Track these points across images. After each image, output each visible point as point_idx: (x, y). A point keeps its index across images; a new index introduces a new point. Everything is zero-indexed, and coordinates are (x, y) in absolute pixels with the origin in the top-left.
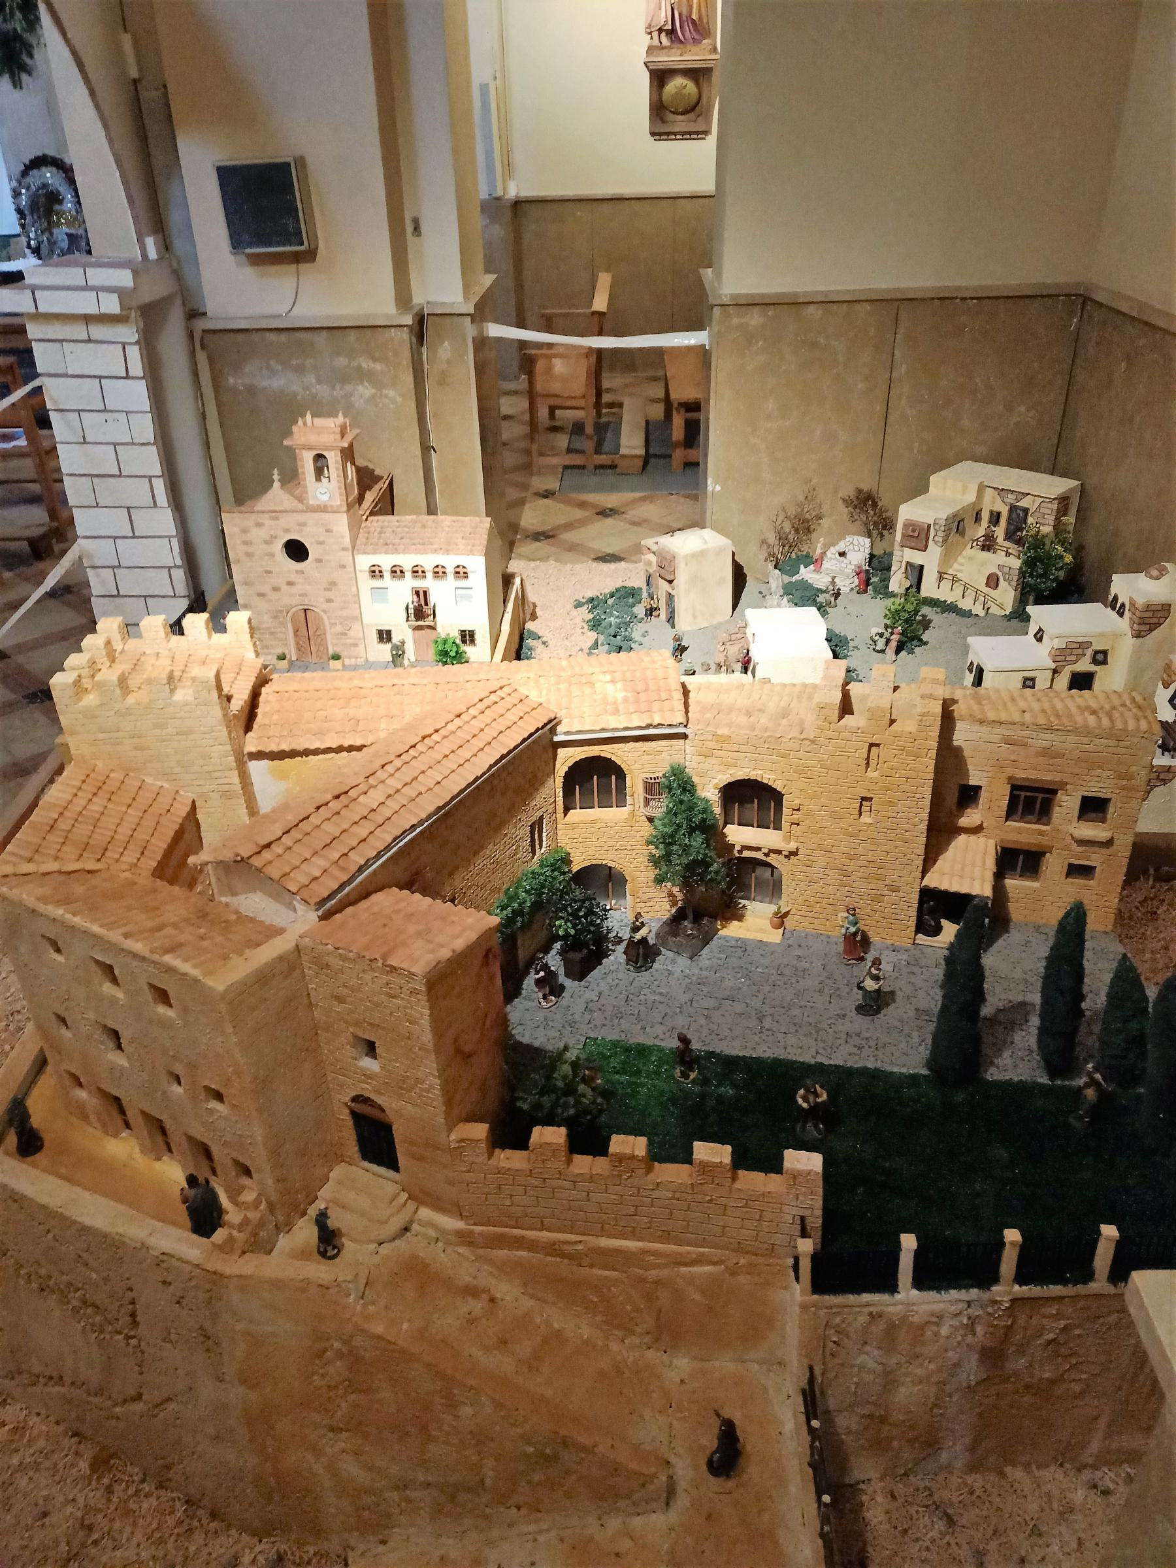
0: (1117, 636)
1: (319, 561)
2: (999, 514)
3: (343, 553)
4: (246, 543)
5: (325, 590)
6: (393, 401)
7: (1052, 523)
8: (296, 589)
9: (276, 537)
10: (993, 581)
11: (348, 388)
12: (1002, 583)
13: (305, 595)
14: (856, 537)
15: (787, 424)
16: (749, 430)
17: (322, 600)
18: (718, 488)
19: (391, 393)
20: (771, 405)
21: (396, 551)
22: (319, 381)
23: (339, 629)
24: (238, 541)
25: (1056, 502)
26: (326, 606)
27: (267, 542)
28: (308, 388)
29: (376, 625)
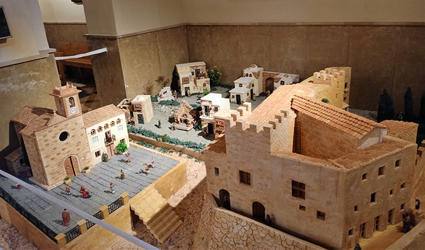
0: (253, 80)
1: (73, 136)
2: (193, 72)
3: (82, 130)
4: (46, 141)
5: (76, 146)
6: (43, 84)
7: (205, 70)
8: (66, 150)
9: (57, 134)
10: (204, 85)
11: (26, 83)
12: (207, 85)
13: (70, 151)
14: (166, 87)
15: (140, 65)
16: (132, 69)
17: (76, 150)
18: (128, 86)
19: (43, 81)
20: (135, 62)
21: (98, 122)
22: (14, 85)
23: (83, 158)
24: (43, 141)
26: (77, 152)
27: (53, 137)
28: (9, 88)
29: (94, 152)
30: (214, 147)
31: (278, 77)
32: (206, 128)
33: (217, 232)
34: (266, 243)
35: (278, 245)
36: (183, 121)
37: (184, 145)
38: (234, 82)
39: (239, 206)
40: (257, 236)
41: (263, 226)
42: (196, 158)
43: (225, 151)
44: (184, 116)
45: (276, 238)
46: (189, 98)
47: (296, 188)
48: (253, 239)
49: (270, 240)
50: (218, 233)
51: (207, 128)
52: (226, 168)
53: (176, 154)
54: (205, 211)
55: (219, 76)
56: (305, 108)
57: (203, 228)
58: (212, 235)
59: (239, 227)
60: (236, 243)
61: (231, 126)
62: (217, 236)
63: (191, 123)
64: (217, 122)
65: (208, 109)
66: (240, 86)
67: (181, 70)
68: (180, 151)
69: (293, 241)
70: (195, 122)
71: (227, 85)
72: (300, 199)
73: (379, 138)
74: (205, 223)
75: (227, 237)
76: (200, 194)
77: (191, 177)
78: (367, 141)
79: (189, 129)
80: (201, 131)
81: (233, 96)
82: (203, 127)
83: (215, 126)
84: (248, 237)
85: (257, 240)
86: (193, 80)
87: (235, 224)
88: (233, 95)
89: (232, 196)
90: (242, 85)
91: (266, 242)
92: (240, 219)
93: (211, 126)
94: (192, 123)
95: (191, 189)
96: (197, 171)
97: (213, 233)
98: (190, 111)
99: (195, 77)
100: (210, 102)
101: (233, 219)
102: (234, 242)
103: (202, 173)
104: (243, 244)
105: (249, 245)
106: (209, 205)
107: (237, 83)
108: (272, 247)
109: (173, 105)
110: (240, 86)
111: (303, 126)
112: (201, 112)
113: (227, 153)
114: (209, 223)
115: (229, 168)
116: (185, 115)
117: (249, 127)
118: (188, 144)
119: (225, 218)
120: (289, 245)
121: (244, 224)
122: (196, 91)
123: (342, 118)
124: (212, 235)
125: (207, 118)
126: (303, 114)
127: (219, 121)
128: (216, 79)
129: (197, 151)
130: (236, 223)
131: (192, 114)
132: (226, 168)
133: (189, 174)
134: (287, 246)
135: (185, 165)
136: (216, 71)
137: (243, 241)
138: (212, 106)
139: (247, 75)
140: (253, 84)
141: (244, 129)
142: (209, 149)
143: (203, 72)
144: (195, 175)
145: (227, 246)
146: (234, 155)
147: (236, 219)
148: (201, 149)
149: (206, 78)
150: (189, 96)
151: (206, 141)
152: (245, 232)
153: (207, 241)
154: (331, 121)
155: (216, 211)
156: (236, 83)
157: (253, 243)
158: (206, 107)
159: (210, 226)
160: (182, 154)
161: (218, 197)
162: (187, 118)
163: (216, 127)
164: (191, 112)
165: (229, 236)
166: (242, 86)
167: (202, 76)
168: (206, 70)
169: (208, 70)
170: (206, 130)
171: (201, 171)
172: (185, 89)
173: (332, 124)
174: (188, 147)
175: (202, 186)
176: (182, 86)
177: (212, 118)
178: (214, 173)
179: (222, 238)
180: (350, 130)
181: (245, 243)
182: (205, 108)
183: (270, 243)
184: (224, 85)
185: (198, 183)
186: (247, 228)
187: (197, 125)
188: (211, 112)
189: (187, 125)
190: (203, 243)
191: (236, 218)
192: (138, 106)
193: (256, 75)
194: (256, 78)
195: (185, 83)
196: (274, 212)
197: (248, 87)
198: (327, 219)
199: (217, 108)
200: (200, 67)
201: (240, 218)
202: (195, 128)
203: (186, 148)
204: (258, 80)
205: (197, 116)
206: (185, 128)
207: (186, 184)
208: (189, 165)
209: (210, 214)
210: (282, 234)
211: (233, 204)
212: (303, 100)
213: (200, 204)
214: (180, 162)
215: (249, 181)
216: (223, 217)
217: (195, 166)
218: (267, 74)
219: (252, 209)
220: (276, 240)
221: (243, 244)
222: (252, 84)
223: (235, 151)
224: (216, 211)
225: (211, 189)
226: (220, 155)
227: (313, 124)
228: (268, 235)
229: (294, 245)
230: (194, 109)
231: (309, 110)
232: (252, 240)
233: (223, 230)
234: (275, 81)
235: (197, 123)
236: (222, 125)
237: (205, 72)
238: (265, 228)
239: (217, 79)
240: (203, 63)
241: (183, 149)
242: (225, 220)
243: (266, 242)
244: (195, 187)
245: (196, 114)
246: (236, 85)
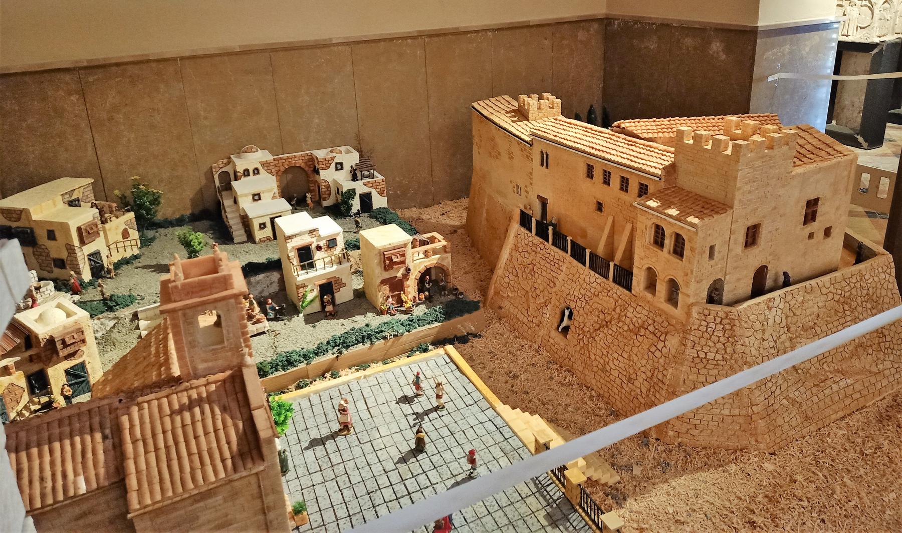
10: (125, 234)
12: (130, 231)
66: (254, 200)
67: (42, 212)
75: (764, 340)
81: (260, 225)
84: (787, 317)
87: (767, 312)
88: (261, 222)
92: (770, 299)
100: (312, 232)
107: (246, 195)
109: (117, 307)
110: (254, 200)
127: (393, 254)
138: (321, 239)
152: (782, 313)
166: (260, 199)
172: (89, 259)
174: (347, 347)
176: (79, 254)
192: (75, 336)
193: (269, 168)
195: (90, 240)
199: (335, 239)
200: (79, 192)
218: (280, 161)
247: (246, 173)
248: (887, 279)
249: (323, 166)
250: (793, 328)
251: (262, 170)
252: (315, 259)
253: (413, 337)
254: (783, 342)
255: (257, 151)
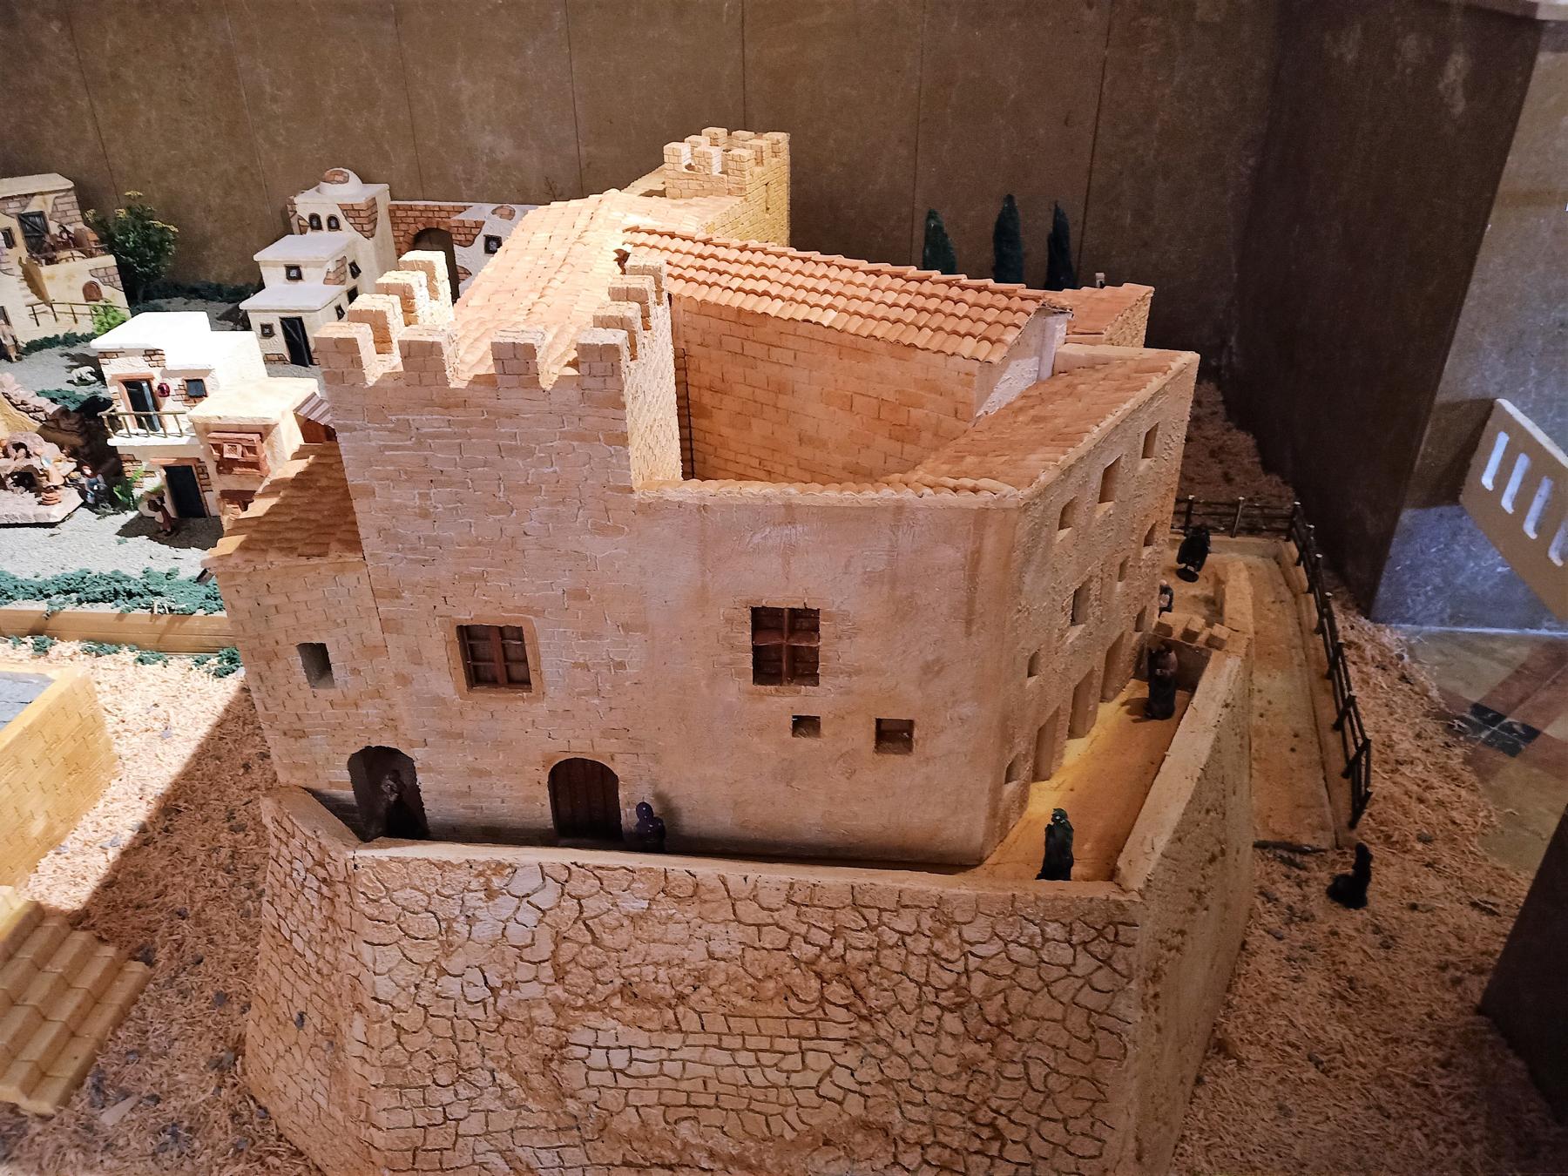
7: (80, 218)
10: (91, 292)
25: (72, 193)
30: (269, 532)
31: (468, 217)
32: (158, 492)
33: (380, 968)
34: (656, 936)
35: (721, 927)
36: (10, 480)
37: (48, 596)
38: (256, 257)
39: (475, 808)
40: (605, 917)
41: (629, 865)
42: (135, 645)
43: (349, 536)
44: (11, 451)
45: (707, 897)
46: (17, 365)
47: (772, 641)
48: (589, 938)
49: (678, 916)
50: (390, 970)
51: (166, 491)
52: (375, 634)
53: (11, 652)
54: (284, 886)
55: (162, 241)
56: (701, 276)
57: (287, 970)
58: (354, 989)
59: (506, 905)
60: (499, 985)
61: (371, 380)
62: (385, 988)
63: (65, 484)
64: (218, 448)
65: (147, 391)
68: (34, 633)
69: (792, 886)
70: (88, 472)
71: (219, 286)
72: (793, 687)
73: (1041, 358)
74: (298, 943)
75: (443, 972)
76: (207, 810)
77: (135, 740)
78: (1005, 376)
79: (55, 513)
80: (131, 515)
82: (137, 493)
83: (211, 468)
84: (560, 939)
85: (607, 939)
86: (19, 271)
88: (265, 322)
89: (429, 769)
90: (302, 269)
91: (658, 931)
92: (499, 867)
93: (183, 479)
94: (69, 482)
95: (150, 798)
96: (162, 708)
97: (356, 978)
98: (38, 425)
99: (25, 255)
100: (151, 354)
101: (463, 876)
102: (486, 983)
103: (193, 708)
104: (536, 978)
105: (567, 973)
106: (304, 848)
107: (275, 264)
108: (690, 946)
110: (289, 278)
111: (698, 370)
112: (109, 417)
113: (364, 543)
114: (325, 935)
115: (387, 625)
116: (18, 446)
117: (488, 367)
118: (74, 588)
119: (418, 883)
120: (771, 910)
121: (521, 885)
122: (49, 328)
123: (888, 289)
124: (354, 989)
125: (155, 440)
126: (695, 309)
127: (226, 441)
128: (153, 259)
129: (138, 611)
130: (482, 895)
131: (58, 435)
132: (375, 634)
133: (120, 728)
134: (764, 916)
135: (87, 689)
136: (139, 216)
137: (534, 963)
139: (315, 223)
140: (353, 265)
141: (458, 380)
142: (243, 548)
143: (70, 229)
144: (157, 725)
145: (451, 1014)
146: (414, 550)
147: (481, 874)
148: (159, 594)
149: (91, 255)
150: (13, 354)
151: (177, 555)
152: (540, 921)
153: (327, 1025)
154: (845, 311)
155: (356, 866)
156: (267, 263)
157: (593, 955)
158: (134, 387)
159: (337, 950)
160: (51, 645)
161: (348, 794)
162: (34, 462)
163: (219, 472)
164: (50, 429)
165: (455, 964)
166: (299, 277)
167: (66, 246)
168: (82, 215)
169: (92, 211)
170: (162, 501)
171: (186, 702)
173: (854, 324)
174: (80, 602)
175: (212, 766)
177: (181, 434)
178: (301, 676)
179: (417, 986)
180: (941, 335)
181: (547, 972)
182: (130, 394)
183: (677, 931)
184: (198, 285)
185: (185, 760)
186: (546, 898)
187: (103, 486)
188: (168, 404)
189: (40, 499)
190: (304, 1041)
191: (481, 869)
193: (358, 220)
194: (362, 231)
196: (664, 786)
197: (331, 276)
198: (921, 742)
201: (499, 864)
202: (92, 507)
203: (69, 608)
204: (376, 245)
205: (88, 443)
206: (31, 514)
207: (114, 782)
208: (106, 687)
209: (319, 892)
210: (734, 872)
211: (436, 805)
212: (677, 243)
213: (225, 852)
214: (53, 681)
215: (516, 671)
216: (403, 887)
217: (143, 685)
219: (548, 802)
220: (707, 906)
221: (536, 978)
222: (350, 261)
223: (420, 521)
224: (356, 866)
225: (296, 766)
226: (322, 570)
227: (750, 348)
228: (662, 894)
229: (794, 903)
230: (64, 412)
231: (724, 280)
232: (584, 945)
233: (416, 946)
234: (459, 237)
235: (100, 477)
236: (250, 457)
237: (81, 225)
238: (641, 870)
239: (156, 258)
240: (58, 182)
241: (49, 616)
242: (420, 895)
243: (658, 931)
244: (170, 780)
245: (81, 435)
246: (266, 273)
247: (315, 222)
248: (1076, 971)
249: (459, 237)
250: (576, 977)
251: (344, 223)
252: (162, 410)
253: (216, 627)
254: (528, 1003)
255: (346, 181)
